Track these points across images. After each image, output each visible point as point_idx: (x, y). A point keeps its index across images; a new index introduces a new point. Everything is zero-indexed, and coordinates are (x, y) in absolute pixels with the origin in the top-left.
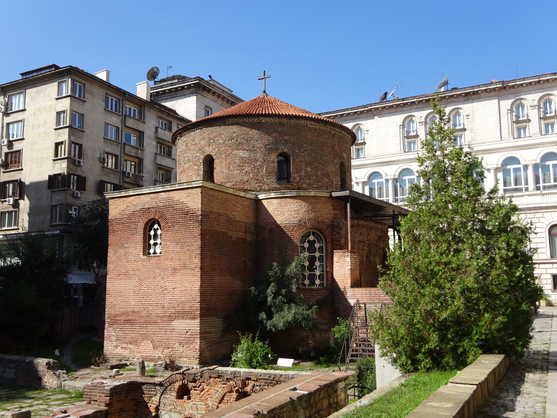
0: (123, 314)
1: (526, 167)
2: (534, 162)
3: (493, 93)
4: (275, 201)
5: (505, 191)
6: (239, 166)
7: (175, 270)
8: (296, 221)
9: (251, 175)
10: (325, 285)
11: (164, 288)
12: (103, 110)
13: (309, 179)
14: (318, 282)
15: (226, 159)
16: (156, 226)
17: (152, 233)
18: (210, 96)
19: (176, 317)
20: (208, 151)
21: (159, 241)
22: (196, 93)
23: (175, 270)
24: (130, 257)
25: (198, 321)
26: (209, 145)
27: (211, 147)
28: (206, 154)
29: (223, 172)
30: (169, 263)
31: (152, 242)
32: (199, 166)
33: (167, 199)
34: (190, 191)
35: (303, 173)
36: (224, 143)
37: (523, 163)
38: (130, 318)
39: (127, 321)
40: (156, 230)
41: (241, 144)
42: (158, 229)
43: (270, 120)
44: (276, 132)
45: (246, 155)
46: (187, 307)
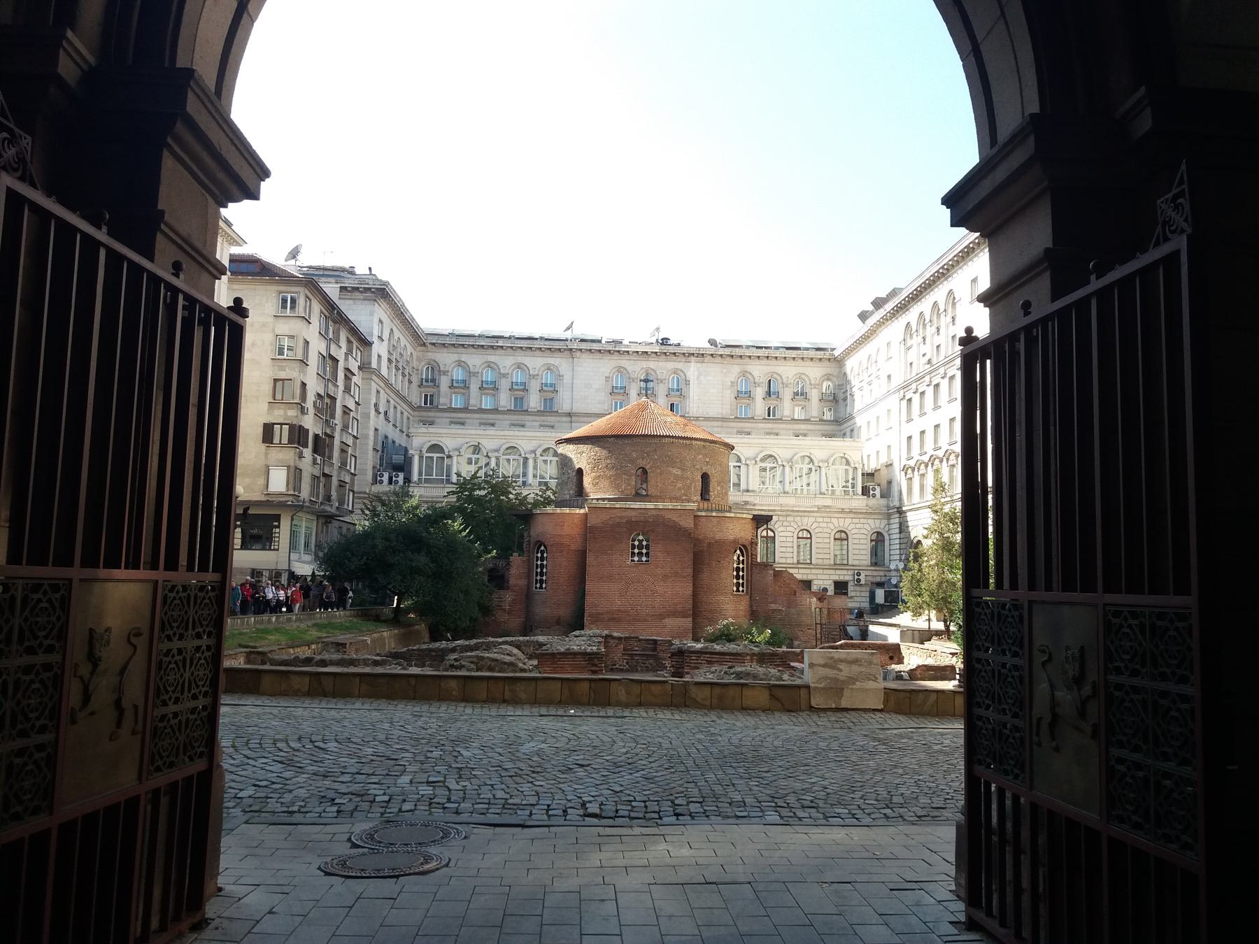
7: (665, 577)
8: (732, 538)
18: (384, 304)
19: (669, 616)
20: (642, 463)
21: (644, 551)
23: (665, 577)
45: (679, 472)
46: (679, 608)
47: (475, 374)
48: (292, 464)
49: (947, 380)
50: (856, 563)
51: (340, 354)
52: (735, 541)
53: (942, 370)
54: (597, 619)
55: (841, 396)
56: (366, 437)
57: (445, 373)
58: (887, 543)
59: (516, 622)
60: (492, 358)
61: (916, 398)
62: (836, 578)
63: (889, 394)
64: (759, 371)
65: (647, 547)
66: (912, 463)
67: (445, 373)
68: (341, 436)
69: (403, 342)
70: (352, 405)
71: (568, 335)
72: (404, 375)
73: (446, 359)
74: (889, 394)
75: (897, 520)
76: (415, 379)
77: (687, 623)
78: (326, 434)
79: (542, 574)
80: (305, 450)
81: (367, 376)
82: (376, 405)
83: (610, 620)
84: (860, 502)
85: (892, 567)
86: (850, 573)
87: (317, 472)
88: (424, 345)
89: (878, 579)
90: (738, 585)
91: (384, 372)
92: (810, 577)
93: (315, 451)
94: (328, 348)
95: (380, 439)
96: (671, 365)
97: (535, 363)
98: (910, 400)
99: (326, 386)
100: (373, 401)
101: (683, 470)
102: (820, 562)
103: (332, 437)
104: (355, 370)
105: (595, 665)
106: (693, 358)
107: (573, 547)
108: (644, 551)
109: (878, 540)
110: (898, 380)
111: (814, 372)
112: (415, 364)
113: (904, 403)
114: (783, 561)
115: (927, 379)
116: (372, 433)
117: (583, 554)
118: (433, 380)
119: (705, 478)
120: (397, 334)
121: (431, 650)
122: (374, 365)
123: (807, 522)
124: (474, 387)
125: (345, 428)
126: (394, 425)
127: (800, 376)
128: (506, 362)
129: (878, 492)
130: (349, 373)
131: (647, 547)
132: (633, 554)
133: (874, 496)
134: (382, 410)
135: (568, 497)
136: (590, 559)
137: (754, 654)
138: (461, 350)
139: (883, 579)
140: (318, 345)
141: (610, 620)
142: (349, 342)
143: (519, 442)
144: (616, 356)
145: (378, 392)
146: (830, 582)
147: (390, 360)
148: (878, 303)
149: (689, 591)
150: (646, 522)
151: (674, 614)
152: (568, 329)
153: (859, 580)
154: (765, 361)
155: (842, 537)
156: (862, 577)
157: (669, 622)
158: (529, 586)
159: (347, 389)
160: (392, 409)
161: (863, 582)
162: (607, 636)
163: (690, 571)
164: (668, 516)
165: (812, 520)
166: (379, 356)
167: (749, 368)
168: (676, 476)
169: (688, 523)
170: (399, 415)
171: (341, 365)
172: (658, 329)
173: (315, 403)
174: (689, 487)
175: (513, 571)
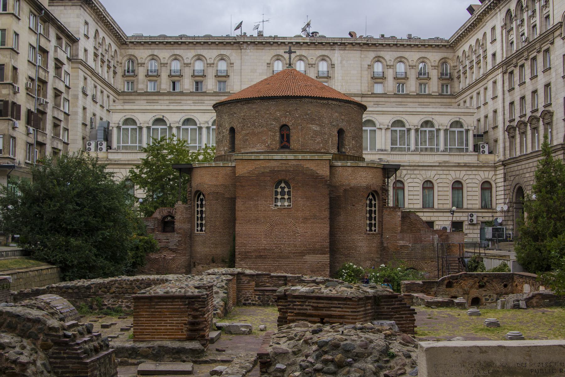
0: (255, 251)
1: (409, 130)
2: (416, 127)
3: (357, 48)
4: (350, 169)
5: (392, 149)
6: (312, 137)
7: (306, 219)
8: (364, 184)
9: (321, 145)
10: (377, 231)
12: (28, 29)
13: (354, 150)
14: (373, 228)
15: (302, 130)
16: (283, 185)
17: (279, 190)
19: (309, 253)
20: (284, 121)
22: (81, 6)
25: (328, 256)
26: (286, 117)
27: (287, 119)
28: (282, 124)
29: (299, 141)
31: (279, 197)
33: (297, 166)
35: (351, 146)
37: (407, 126)
38: (262, 254)
39: (261, 257)
40: (283, 188)
41: (313, 120)
42: (285, 187)
43: (334, 103)
44: (337, 112)
45: (318, 128)
46: (318, 246)
47: (165, 64)
48: (6, 133)
49: (542, 53)
50: (470, 206)
51: (50, 45)
52: (367, 187)
53: (537, 46)
54: (246, 256)
55: (456, 75)
56: (76, 113)
57: (142, 64)
58: (494, 190)
59: (182, 260)
60: (177, 52)
61: (517, 71)
62: (454, 219)
63: (494, 70)
64: (389, 55)
65: (289, 193)
66: (515, 124)
67: (142, 64)
68: (53, 111)
69: (108, 41)
70: (61, 87)
71: (238, 32)
72: (109, 67)
73: (142, 54)
74: (494, 70)
75: (502, 171)
76: (120, 71)
77: (325, 259)
78: (38, 110)
79: (202, 219)
80: (17, 122)
81: (75, 65)
82: (83, 88)
83: (257, 257)
84: (471, 159)
85: (499, 209)
86: (467, 214)
87: (31, 140)
88: (125, 44)
89: (487, 219)
90: (370, 225)
91: (91, 62)
92: (433, 219)
93: (28, 122)
94: (38, 41)
95: (89, 115)
97: (211, 54)
98: (511, 73)
99: (37, 72)
100: (81, 84)
101: (320, 125)
102: (441, 206)
103: (44, 113)
104: (65, 61)
105: (196, 310)
106: (337, 47)
107: (227, 195)
108: (286, 197)
109: (486, 187)
110: (499, 60)
111: (434, 57)
112: (119, 58)
113: (507, 76)
114: (411, 206)
115: (525, 54)
116: (80, 110)
117: (232, 201)
118: (133, 71)
119: (341, 132)
120: (102, 34)
121: (68, 288)
122: (81, 56)
123: (430, 175)
125: (57, 106)
126: (102, 106)
127: (423, 60)
129: (486, 149)
130: (59, 64)
132: (276, 199)
133: (483, 152)
134: (89, 93)
135: (223, 153)
136: (239, 204)
137: (368, 298)
138: (153, 46)
139: (491, 219)
140: (27, 39)
141: (257, 257)
142: (59, 38)
143: (195, 115)
145: (85, 79)
146: (449, 223)
147: (96, 55)
149: (327, 231)
150: (287, 171)
151: (314, 251)
152: (237, 28)
153: (472, 220)
154: (394, 48)
155: (457, 186)
156: (474, 218)
157: (308, 258)
158: (192, 229)
159: (58, 76)
160: (99, 93)
161: (475, 222)
162: (239, 274)
163: (327, 214)
164: (307, 165)
165: (434, 173)
166: (86, 50)
167: (382, 54)
168: (316, 133)
169: (324, 171)
170: (105, 98)
171: (51, 55)
172: (308, 25)
173: (27, 84)
174: (327, 142)
175: (177, 217)
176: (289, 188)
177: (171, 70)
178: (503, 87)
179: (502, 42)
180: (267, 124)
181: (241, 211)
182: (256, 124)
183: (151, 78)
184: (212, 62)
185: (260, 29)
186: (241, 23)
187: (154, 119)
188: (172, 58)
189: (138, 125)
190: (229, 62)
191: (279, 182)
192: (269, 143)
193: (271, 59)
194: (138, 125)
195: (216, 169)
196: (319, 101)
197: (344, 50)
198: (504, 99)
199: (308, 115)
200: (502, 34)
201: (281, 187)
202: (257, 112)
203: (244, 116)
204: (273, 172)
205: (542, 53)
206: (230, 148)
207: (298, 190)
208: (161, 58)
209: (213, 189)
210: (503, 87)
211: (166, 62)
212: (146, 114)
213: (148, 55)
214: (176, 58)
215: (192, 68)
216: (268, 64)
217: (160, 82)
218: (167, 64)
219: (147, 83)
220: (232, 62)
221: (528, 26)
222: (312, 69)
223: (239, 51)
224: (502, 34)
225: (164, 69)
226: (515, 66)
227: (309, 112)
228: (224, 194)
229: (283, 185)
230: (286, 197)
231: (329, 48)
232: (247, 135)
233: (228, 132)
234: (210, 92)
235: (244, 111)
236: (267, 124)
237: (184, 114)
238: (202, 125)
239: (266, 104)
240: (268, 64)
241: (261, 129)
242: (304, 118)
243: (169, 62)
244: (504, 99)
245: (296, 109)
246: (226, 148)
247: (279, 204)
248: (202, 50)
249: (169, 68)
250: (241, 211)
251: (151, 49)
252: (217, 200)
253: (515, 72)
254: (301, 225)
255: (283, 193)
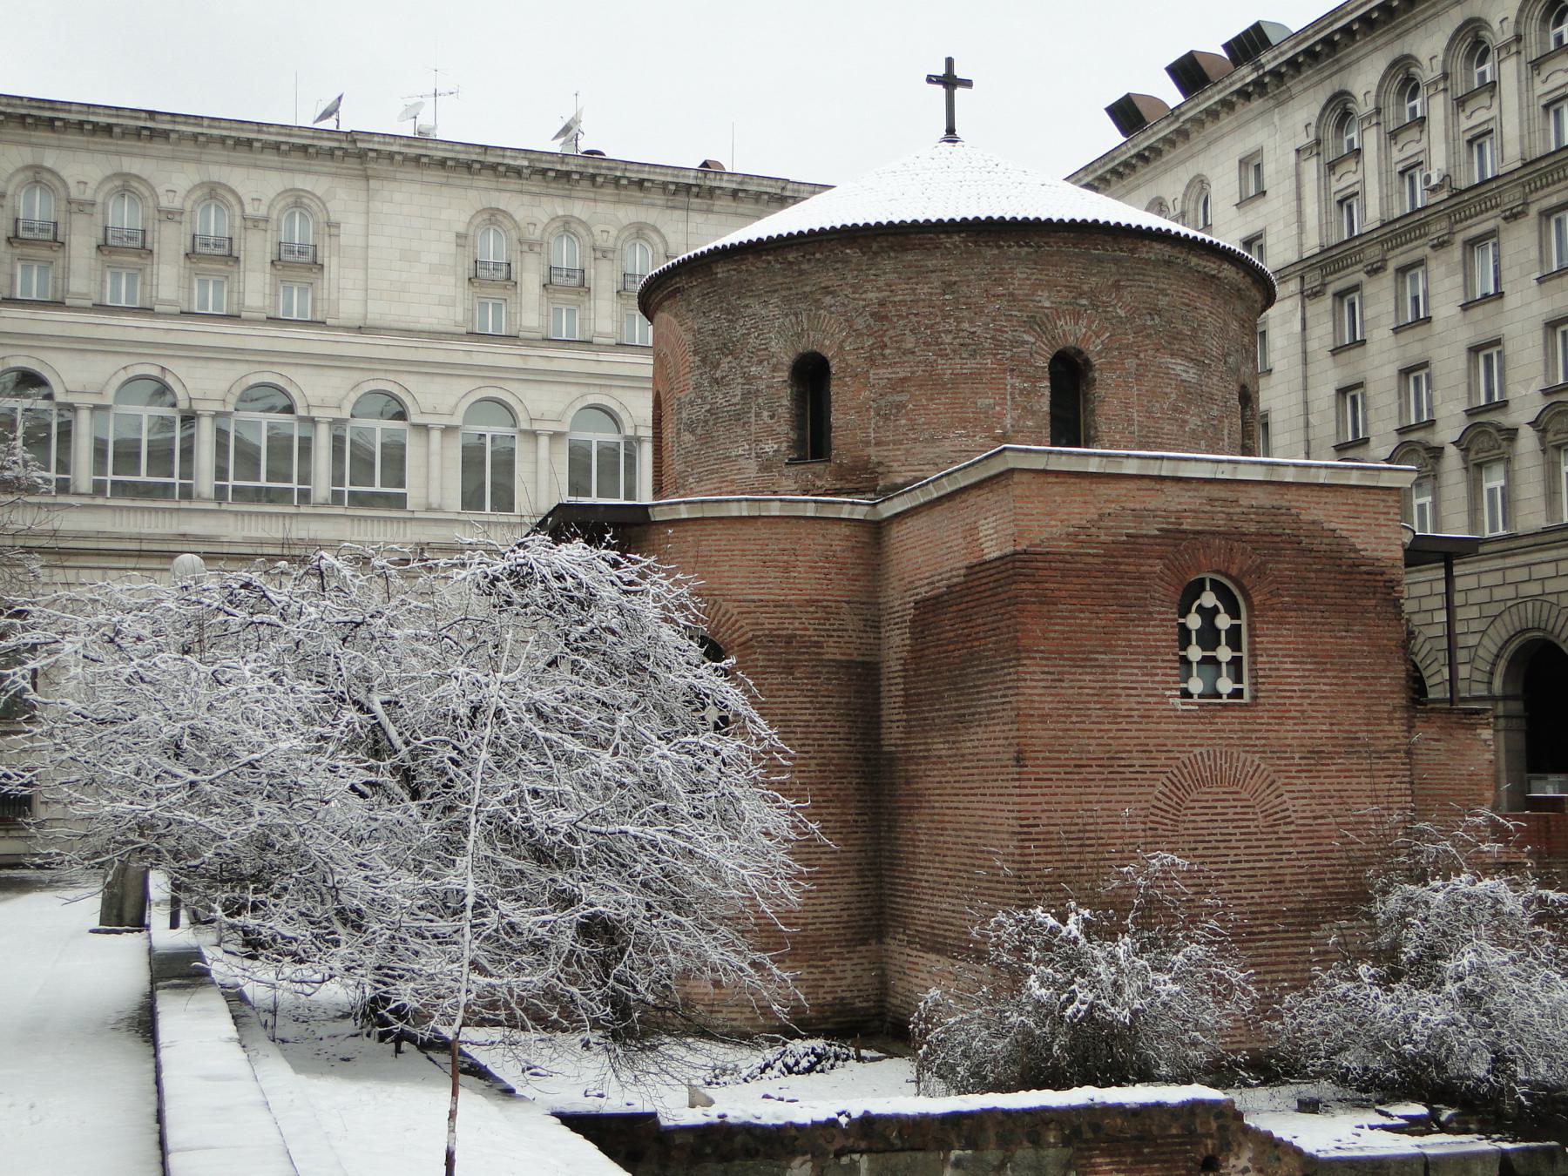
11: (1277, 819)
16: (1209, 599)
20: (1072, 332)
24: (1124, 703)
26: (1077, 316)
27: (1083, 322)
29: (1130, 420)
30: (1290, 734)
32: (1034, 380)
34: (1359, 496)
36: (1130, 320)
40: (1208, 615)
41: (1177, 336)
42: (1215, 610)
47: (85, 207)
60: (133, 165)
96: (627, 214)
97: (258, 186)
101: (1197, 363)
107: (832, 652)
115: (1438, 229)
124: (81, 244)
128: (175, 179)
131: (1234, 632)
132: (1185, 661)
144: (483, 181)
148: (1189, 72)
150: (1233, 535)
152: (326, 115)
176: (1234, 612)
177: (106, 228)
178: (1304, 341)
179: (1299, 198)
180: (999, 344)
181: (1043, 718)
182: (948, 339)
183: (29, 251)
184: (263, 211)
185: (425, 120)
186: (340, 99)
187: (123, 376)
188: (110, 185)
189: (60, 397)
190: (322, 218)
191: (1197, 588)
192: (1008, 422)
193: (470, 222)
194: (60, 397)
195: (782, 529)
196: (1194, 261)
197: (709, 211)
198: (1305, 378)
199: (1159, 313)
200: (1298, 175)
201: (1200, 609)
202: (948, 286)
203: (882, 304)
204: (1174, 536)
205: (1530, 222)
206: (798, 445)
207: (1281, 622)
208: (71, 183)
209: (768, 623)
210: (1304, 341)
211: (88, 196)
212: (89, 356)
213: (20, 164)
214: (126, 186)
215: (186, 228)
216: (458, 235)
217: (66, 271)
218: (93, 204)
219: (13, 268)
220: (333, 218)
221: (1450, 140)
222: (604, 266)
223: (361, 183)
224: (1298, 175)
225: (79, 221)
226: (1375, 270)
227: (1163, 302)
228: (818, 645)
229: (1209, 599)
230: (1224, 654)
231: (659, 202)
232: (899, 384)
233: (784, 375)
234: (255, 315)
235: (886, 278)
236: (999, 344)
237: (242, 369)
238: (314, 413)
239: (991, 253)
240: (458, 235)
241: (971, 364)
242: (1145, 327)
243: (100, 199)
244: (1305, 378)
245: (1117, 286)
246: (770, 447)
247: (1196, 685)
248: (226, 170)
249: (99, 218)
250: (1043, 718)
251: (30, 144)
252: (789, 669)
253: (1368, 290)
254: (1299, 785)
255: (1209, 637)
